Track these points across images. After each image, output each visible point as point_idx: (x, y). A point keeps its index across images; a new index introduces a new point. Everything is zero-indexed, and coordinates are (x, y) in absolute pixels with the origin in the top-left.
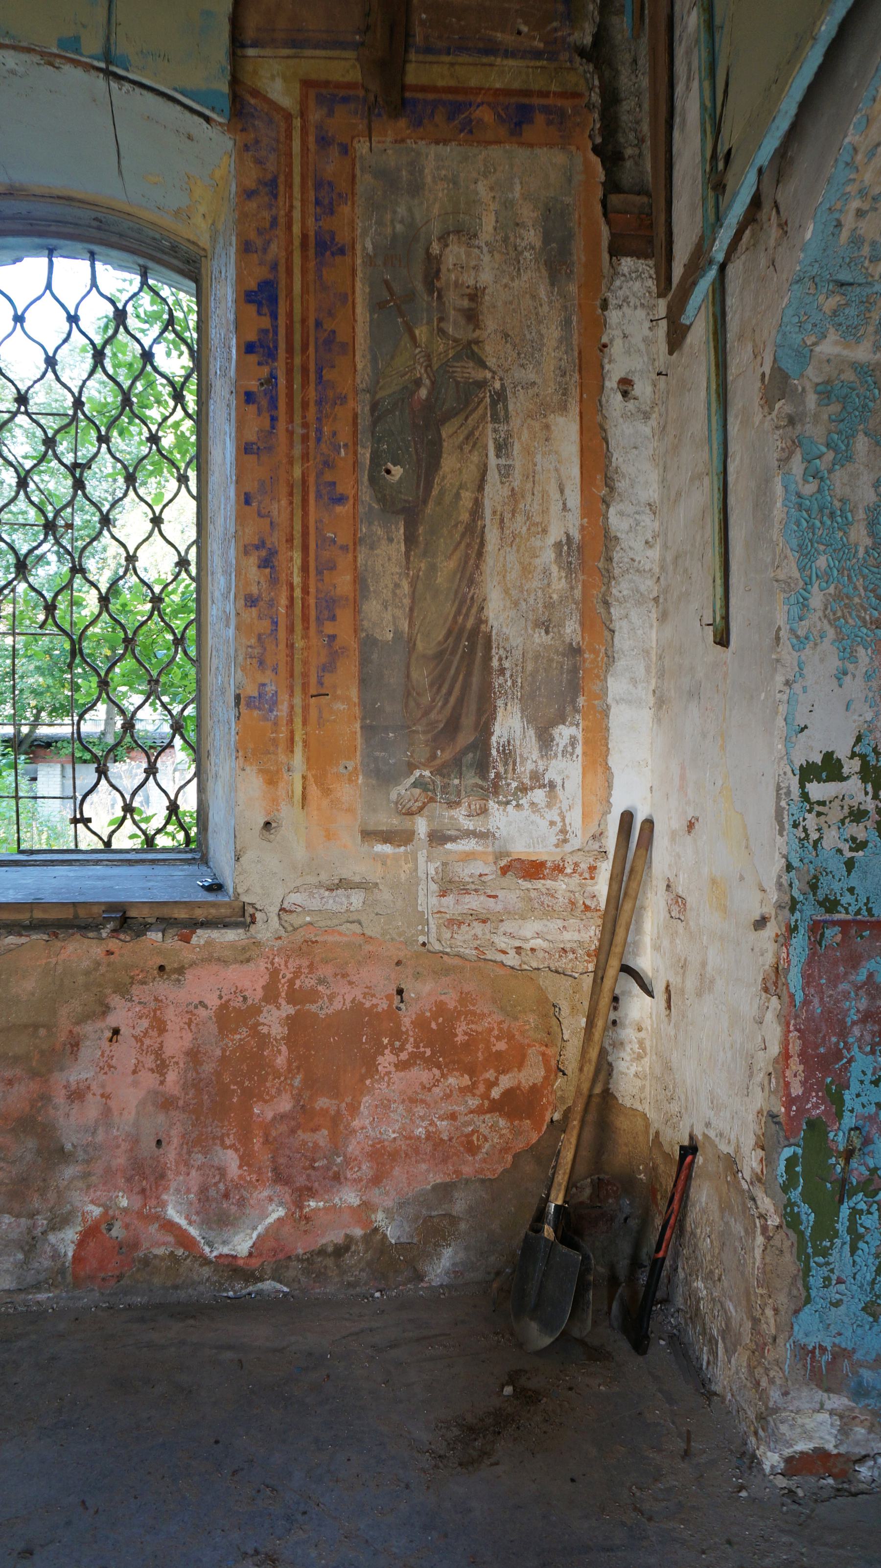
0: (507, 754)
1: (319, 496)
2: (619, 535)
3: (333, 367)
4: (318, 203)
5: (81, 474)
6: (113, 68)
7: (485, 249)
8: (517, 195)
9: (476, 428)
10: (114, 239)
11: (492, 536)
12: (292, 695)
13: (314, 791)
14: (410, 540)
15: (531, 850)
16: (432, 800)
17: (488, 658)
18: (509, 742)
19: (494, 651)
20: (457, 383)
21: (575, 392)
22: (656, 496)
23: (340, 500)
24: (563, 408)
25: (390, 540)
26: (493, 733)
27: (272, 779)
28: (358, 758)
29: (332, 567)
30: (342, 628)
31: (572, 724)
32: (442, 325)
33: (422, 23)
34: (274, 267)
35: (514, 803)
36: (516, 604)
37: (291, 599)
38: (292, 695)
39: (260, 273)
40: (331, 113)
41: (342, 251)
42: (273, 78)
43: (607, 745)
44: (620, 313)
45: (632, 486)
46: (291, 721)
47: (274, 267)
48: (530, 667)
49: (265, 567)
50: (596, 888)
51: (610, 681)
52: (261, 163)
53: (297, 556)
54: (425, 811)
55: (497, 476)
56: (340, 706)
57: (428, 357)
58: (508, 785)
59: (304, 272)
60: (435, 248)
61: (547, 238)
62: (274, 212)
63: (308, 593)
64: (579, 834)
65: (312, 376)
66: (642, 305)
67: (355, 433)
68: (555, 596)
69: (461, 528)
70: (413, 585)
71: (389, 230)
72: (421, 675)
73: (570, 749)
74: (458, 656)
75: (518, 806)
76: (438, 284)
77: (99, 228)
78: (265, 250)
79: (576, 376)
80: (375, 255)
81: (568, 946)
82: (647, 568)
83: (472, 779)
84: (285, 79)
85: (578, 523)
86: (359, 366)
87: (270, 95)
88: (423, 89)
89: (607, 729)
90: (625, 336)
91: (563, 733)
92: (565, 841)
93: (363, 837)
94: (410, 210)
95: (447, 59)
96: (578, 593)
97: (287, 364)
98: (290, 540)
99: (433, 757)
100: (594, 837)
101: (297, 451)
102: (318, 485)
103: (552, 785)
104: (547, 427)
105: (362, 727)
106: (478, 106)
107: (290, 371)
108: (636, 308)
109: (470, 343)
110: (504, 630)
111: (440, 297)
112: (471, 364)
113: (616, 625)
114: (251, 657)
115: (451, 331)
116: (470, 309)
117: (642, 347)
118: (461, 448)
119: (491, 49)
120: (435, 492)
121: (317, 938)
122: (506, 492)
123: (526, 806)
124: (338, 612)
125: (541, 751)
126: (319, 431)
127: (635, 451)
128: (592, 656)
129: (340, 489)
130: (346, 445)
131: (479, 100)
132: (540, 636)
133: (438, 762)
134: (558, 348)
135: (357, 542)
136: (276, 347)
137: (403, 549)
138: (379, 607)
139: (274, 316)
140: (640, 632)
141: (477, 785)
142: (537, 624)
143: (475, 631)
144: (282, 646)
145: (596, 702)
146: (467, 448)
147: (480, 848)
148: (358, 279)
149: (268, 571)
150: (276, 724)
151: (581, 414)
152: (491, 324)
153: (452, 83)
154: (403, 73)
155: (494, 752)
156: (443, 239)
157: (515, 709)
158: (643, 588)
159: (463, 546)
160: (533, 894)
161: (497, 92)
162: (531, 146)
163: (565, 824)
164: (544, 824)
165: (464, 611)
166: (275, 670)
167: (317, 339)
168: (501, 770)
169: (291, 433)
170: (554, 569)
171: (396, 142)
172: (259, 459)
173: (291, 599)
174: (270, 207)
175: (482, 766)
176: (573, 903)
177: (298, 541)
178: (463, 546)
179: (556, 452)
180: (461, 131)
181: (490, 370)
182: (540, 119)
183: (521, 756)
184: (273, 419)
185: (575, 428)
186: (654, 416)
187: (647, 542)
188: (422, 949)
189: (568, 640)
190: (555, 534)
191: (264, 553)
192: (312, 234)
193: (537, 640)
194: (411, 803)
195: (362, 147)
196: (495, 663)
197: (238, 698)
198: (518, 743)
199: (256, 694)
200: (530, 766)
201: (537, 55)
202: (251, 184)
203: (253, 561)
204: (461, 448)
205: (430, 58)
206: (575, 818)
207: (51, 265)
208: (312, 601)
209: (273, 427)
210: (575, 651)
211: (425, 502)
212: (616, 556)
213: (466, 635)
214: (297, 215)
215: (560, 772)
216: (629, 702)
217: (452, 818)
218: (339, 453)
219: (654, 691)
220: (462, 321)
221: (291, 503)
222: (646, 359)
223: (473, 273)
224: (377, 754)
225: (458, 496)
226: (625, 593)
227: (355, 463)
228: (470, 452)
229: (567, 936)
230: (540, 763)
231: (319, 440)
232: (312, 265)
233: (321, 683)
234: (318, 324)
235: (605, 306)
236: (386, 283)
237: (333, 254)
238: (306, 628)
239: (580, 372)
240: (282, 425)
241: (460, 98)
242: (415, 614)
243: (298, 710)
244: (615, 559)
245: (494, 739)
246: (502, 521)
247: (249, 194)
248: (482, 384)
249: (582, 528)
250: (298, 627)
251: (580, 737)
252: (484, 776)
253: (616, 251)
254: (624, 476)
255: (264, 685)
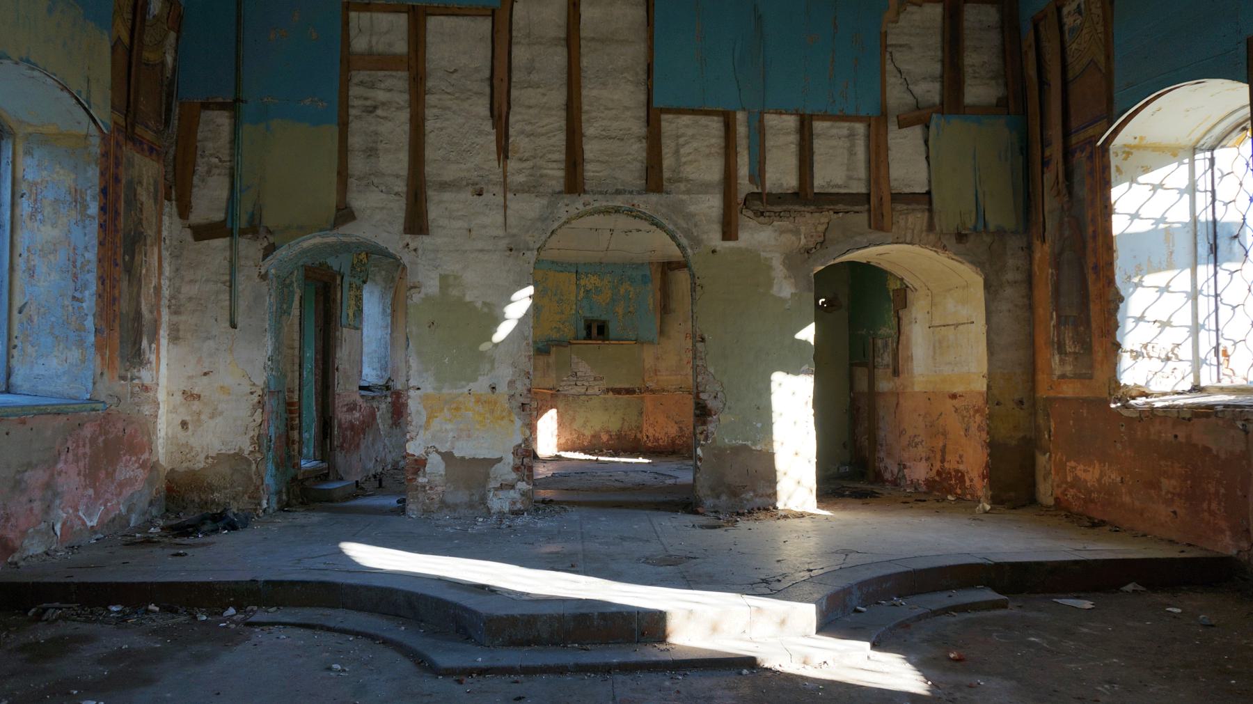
53: (109, 282)
60: (136, 186)
156: (137, 183)
164: (149, 374)
248: (142, 233)
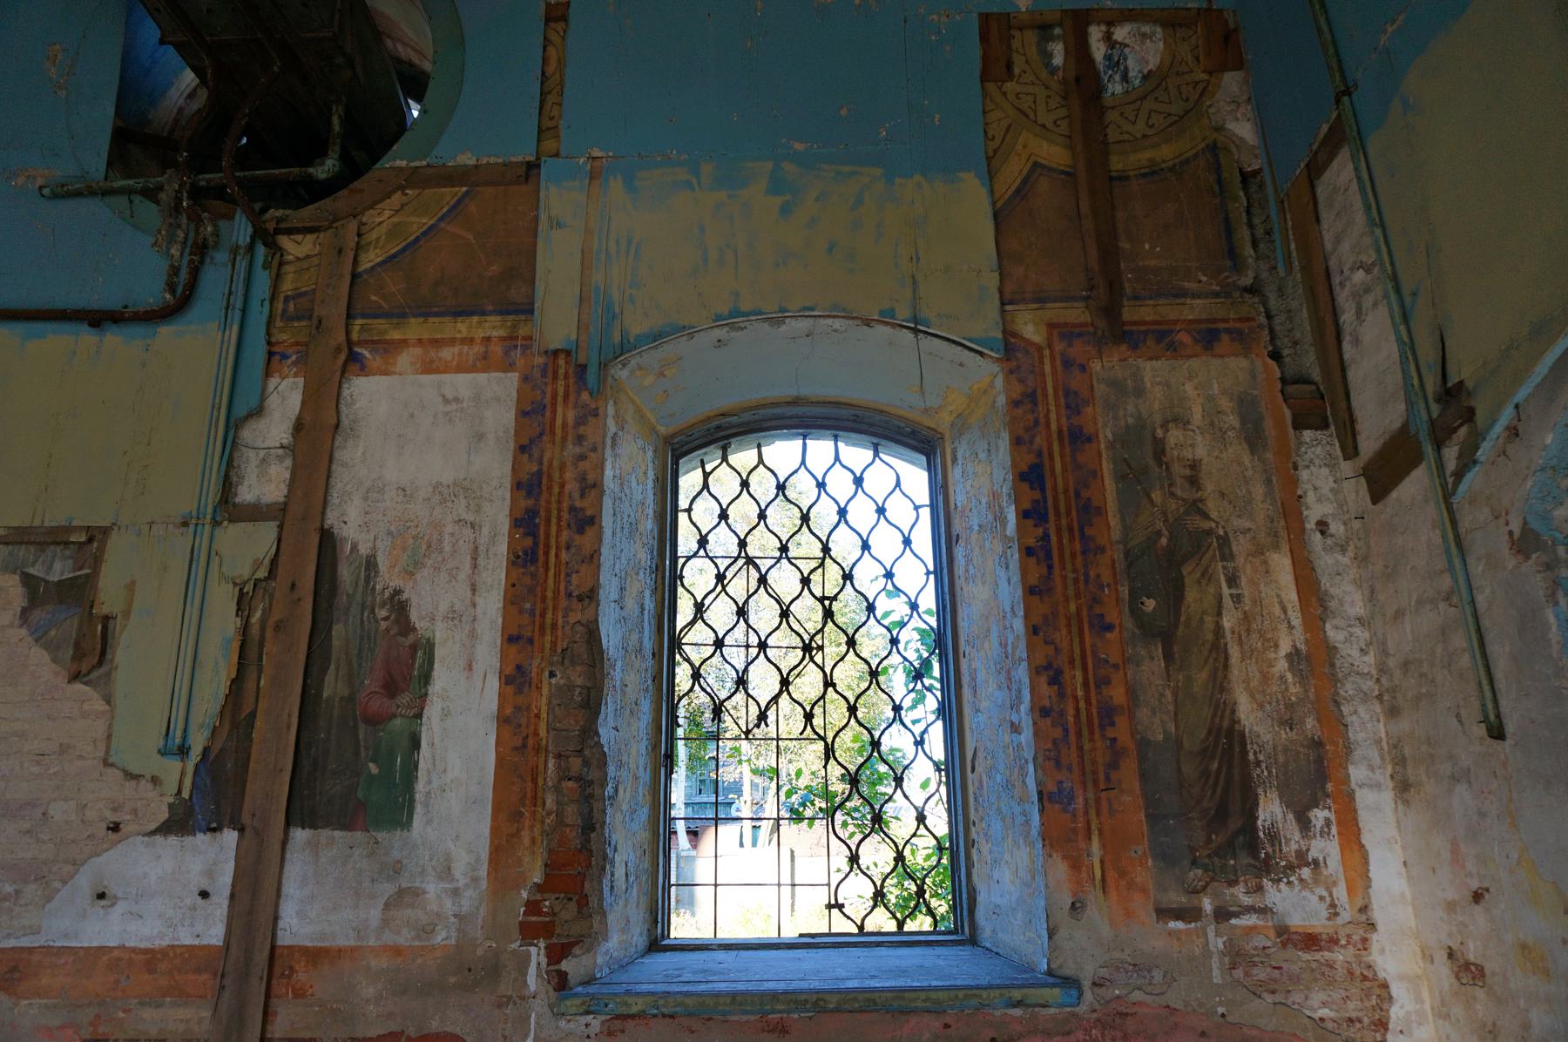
0: (1273, 836)
1: (1091, 626)
2: (1337, 644)
3: (1092, 525)
4: (1068, 406)
5: (830, 605)
6: (920, 327)
7: (1197, 431)
8: (1216, 392)
9: (1208, 566)
10: (865, 427)
11: (1234, 652)
12: (1085, 791)
13: (1112, 875)
14: (1168, 657)
15: (1307, 923)
16: (1213, 879)
17: (1244, 753)
18: (1272, 824)
19: (1249, 746)
20: (1190, 532)
21: (1284, 534)
22: (1362, 611)
23: (1110, 628)
24: (1277, 547)
25: (1152, 658)
26: (1257, 818)
27: (1075, 864)
28: (1146, 843)
29: (1107, 681)
30: (1121, 731)
31: (1324, 808)
32: (1173, 489)
33: (1128, 279)
34: (1040, 454)
35: (1285, 880)
36: (1261, 706)
37: (1077, 709)
38: (1085, 791)
39: (1029, 459)
40: (1070, 345)
41: (1089, 440)
42: (1026, 323)
43: (1357, 825)
44: (1309, 472)
45: (1342, 605)
46: (1086, 813)
47: (1040, 454)
48: (1281, 759)
49: (1054, 684)
50: (1371, 958)
51: (1352, 769)
52: (1023, 382)
53: (1079, 674)
54: (1209, 890)
55: (1231, 603)
56: (1127, 798)
57: (1164, 513)
58: (1278, 863)
59: (1062, 456)
60: (1160, 433)
61: (1244, 421)
62: (1036, 415)
63: (1090, 704)
64: (1347, 907)
65: (1077, 534)
66: (1325, 464)
67: (1115, 574)
68: (1293, 699)
69: (1208, 646)
70: (1175, 694)
71: (1123, 423)
72: (1190, 770)
73: (1326, 830)
74: (1219, 752)
75: (1289, 883)
76: (1165, 459)
77: (855, 421)
78: (1031, 442)
79: (1282, 522)
80: (1114, 441)
81: (1354, 1015)
82: (1366, 671)
83: (1245, 860)
84: (1036, 324)
85: (1302, 638)
86: (1112, 524)
87: (1026, 336)
88: (1136, 323)
89: (1355, 811)
90: (1316, 489)
91: (1319, 816)
92: (1336, 914)
93: (1157, 915)
94: (1136, 407)
95: (1151, 302)
96: (1311, 695)
97: (1056, 525)
98: (1072, 662)
99: (1209, 841)
100: (1360, 910)
101: (1071, 591)
102: (1089, 616)
103: (1316, 862)
104: (1265, 562)
105: (1146, 816)
106: (1178, 332)
107: (1059, 531)
108: (1320, 467)
109: (1195, 502)
110: (1255, 728)
111: (1167, 469)
112: (1198, 517)
113: (1349, 720)
114: (1049, 759)
115: (1179, 493)
116: (1192, 476)
117: (1331, 496)
118: (1199, 582)
119: (1182, 294)
120: (1183, 619)
121: (1128, 1011)
122: (1239, 615)
123: (1296, 882)
124: (1116, 719)
125: (1301, 833)
126: (1086, 574)
127: (1339, 577)
128: (1333, 748)
129: (1108, 620)
130: (1108, 585)
131: (1178, 327)
132: (1286, 733)
133: (1213, 845)
134: (1264, 501)
135: (1126, 661)
136: (1047, 513)
137: (1163, 665)
138: (1149, 714)
139: (1043, 490)
140: (1369, 725)
141: (1250, 865)
142: (1282, 723)
143: (1230, 732)
144: (1073, 748)
145: (1342, 787)
146: (1204, 582)
147: (1261, 923)
148: (1104, 460)
149: (1056, 687)
150: (1074, 815)
151: (1291, 550)
152: (1209, 487)
153: (1157, 318)
154: (1120, 314)
155: (1261, 834)
156: (1164, 426)
157: (1274, 795)
158: (1365, 688)
159: (1211, 660)
160: (1314, 965)
161: (1190, 321)
162: (1222, 356)
163: (1333, 899)
164: (1314, 899)
165: (1219, 713)
166: (1070, 769)
167: (1077, 506)
168: (1270, 850)
169: (1064, 578)
170: (1289, 676)
171: (1121, 360)
172: (1041, 598)
173: (1077, 709)
174: (1033, 412)
175: (1253, 846)
176: (1351, 973)
177: (1078, 663)
178: (1211, 660)
179: (1276, 582)
180: (1167, 350)
181: (1214, 521)
182: (1225, 338)
183: (1285, 837)
184: (1050, 567)
185: (1287, 562)
186: (1350, 548)
187: (1362, 650)
188: (1221, 1020)
189: (1310, 736)
190: (1285, 647)
191: (1052, 673)
192: (1065, 429)
193: (1284, 736)
194: (1195, 883)
195: (1096, 366)
196: (1251, 757)
197: (1040, 793)
198: (1281, 826)
199: (1056, 790)
200: (1294, 847)
201: (1216, 295)
202: (1015, 396)
203: (1043, 679)
204: (1199, 582)
205: (1137, 303)
206: (1341, 893)
207: (805, 445)
208: (1094, 711)
209: (1050, 573)
210: (1317, 744)
211: (1176, 627)
212: (1338, 663)
213: (1223, 734)
214: (1053, 416)
215: (1322, 851)
216: (1370, 786)
217: (1232, 895)
218: (1104, 591)
219: (1392, 776)
220: (1187, 486)
221: (1070, 632)
222: (1335, 504)
223: (1190, 449)
224: (1162, 839)
225: (1201, 621)
226: (1351, 692)
227: (1117, 600)
228: (1207, 585)
229: (1351, 1005)
230: (1302, 842)
231: (1086, 581)
232: (1068, 450)
233: (1108, 779)
234: (1077, 494)
235: (1296, 468)
236: (1125, 460)
237: (1083, 442)
238: (1092, 733)
239: (1285, 518)
240: (1057, 571)
241: (1164, 327)
242: (1180, 717)
243: (1092, 802)
244: (1338, 665)
245: (1259, 823)
246: (1240, 638)
247: (1015, 404)
248: (1209, 532)
249: (1307, 641)
250: (1085, 732)
251: (1333, 818)
252: (1256, 856)
253: (1298, 425)
254: (1333, 597)
255: (1061, 782)
